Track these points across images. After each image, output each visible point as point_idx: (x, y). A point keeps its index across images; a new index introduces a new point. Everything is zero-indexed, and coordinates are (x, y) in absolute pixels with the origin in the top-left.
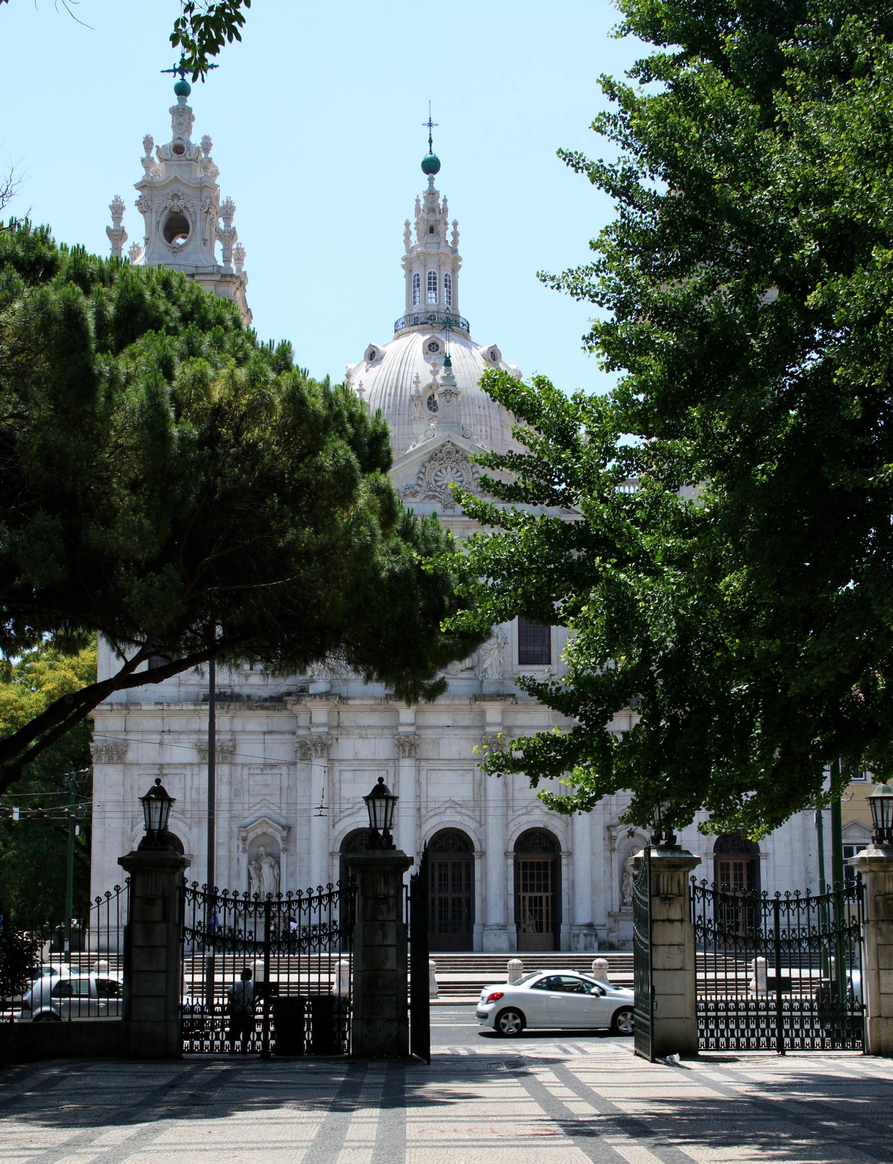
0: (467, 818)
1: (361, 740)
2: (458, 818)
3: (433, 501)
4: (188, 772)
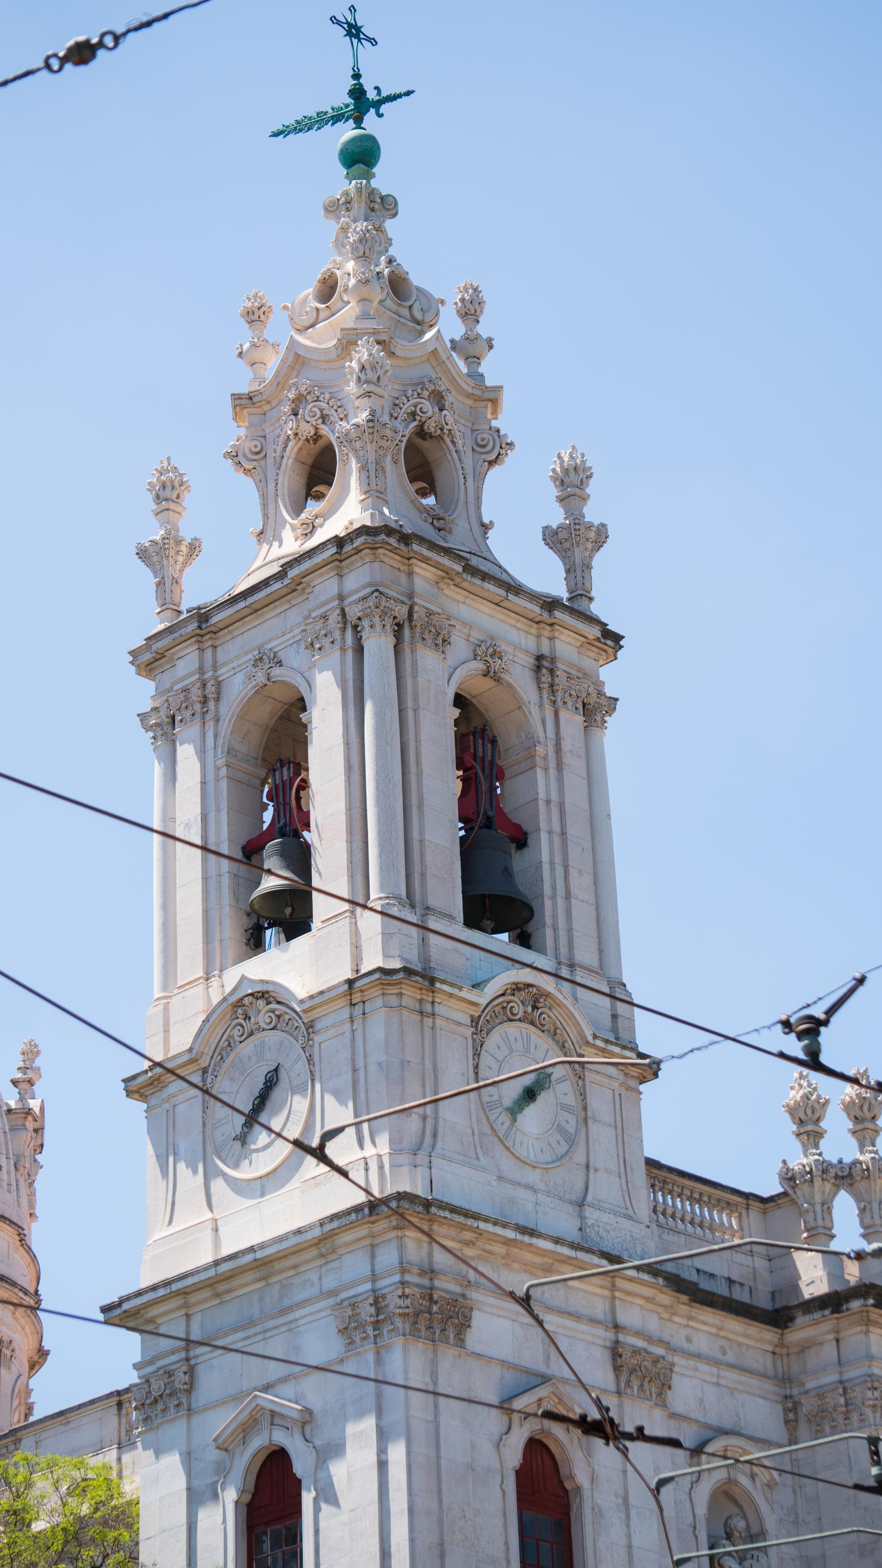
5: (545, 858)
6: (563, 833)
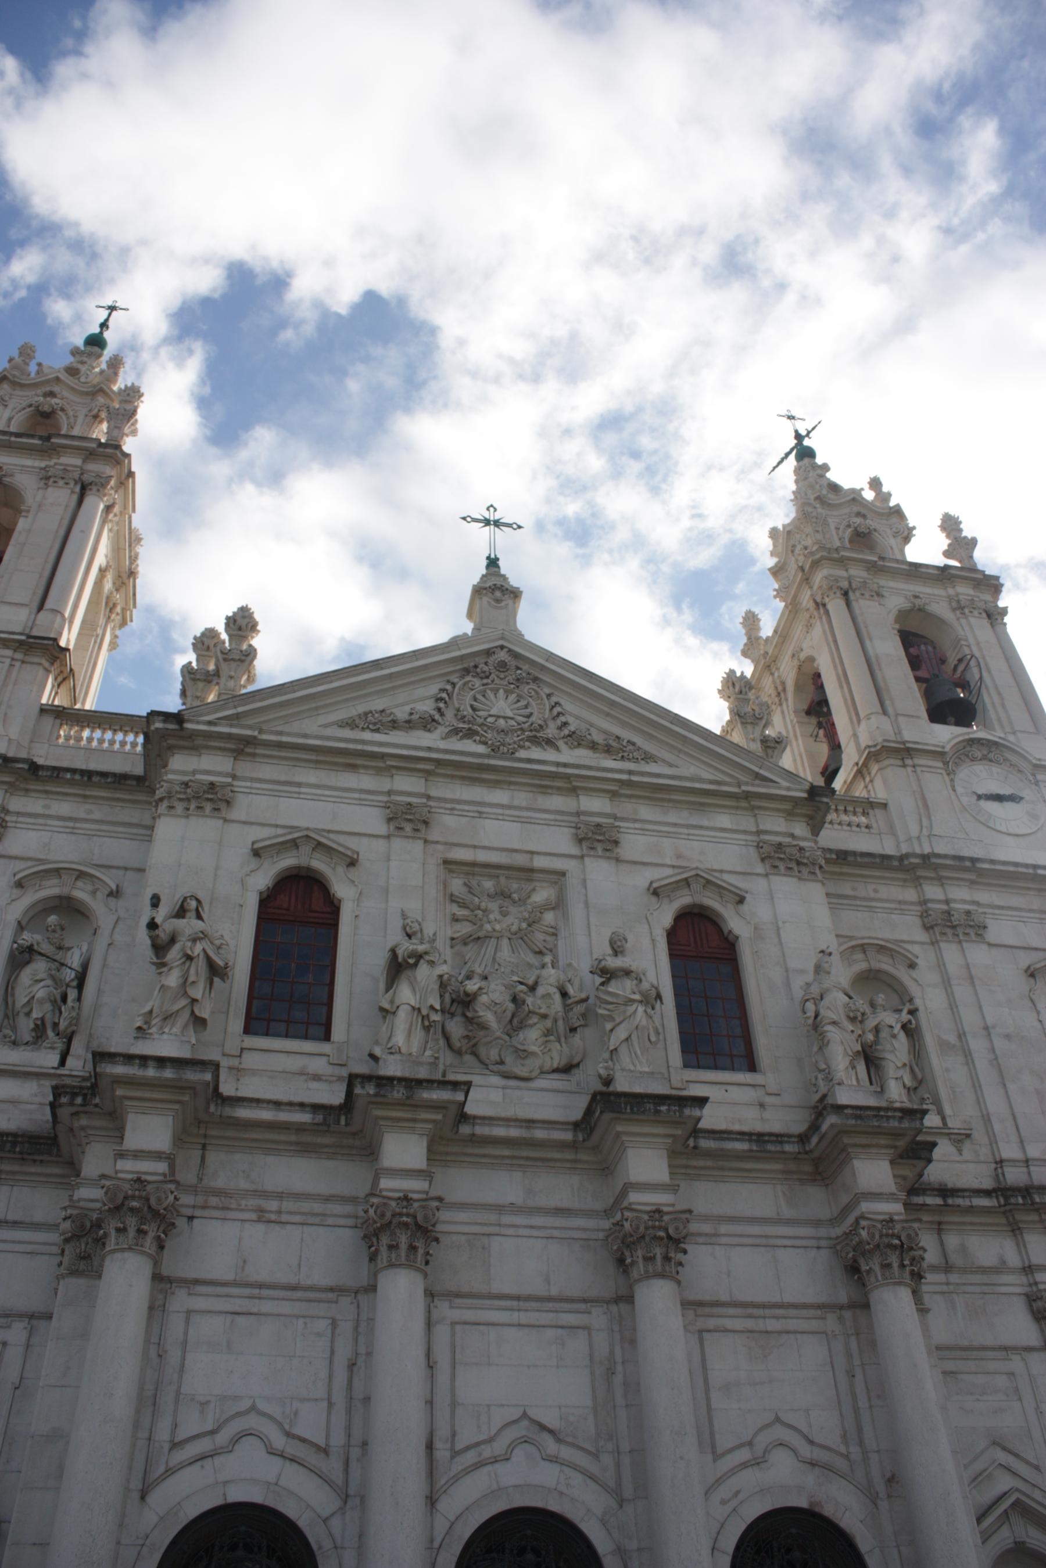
0: (577, 1479)
1: (261, 1227)
2: (548, 1475)
3: (465, 741)
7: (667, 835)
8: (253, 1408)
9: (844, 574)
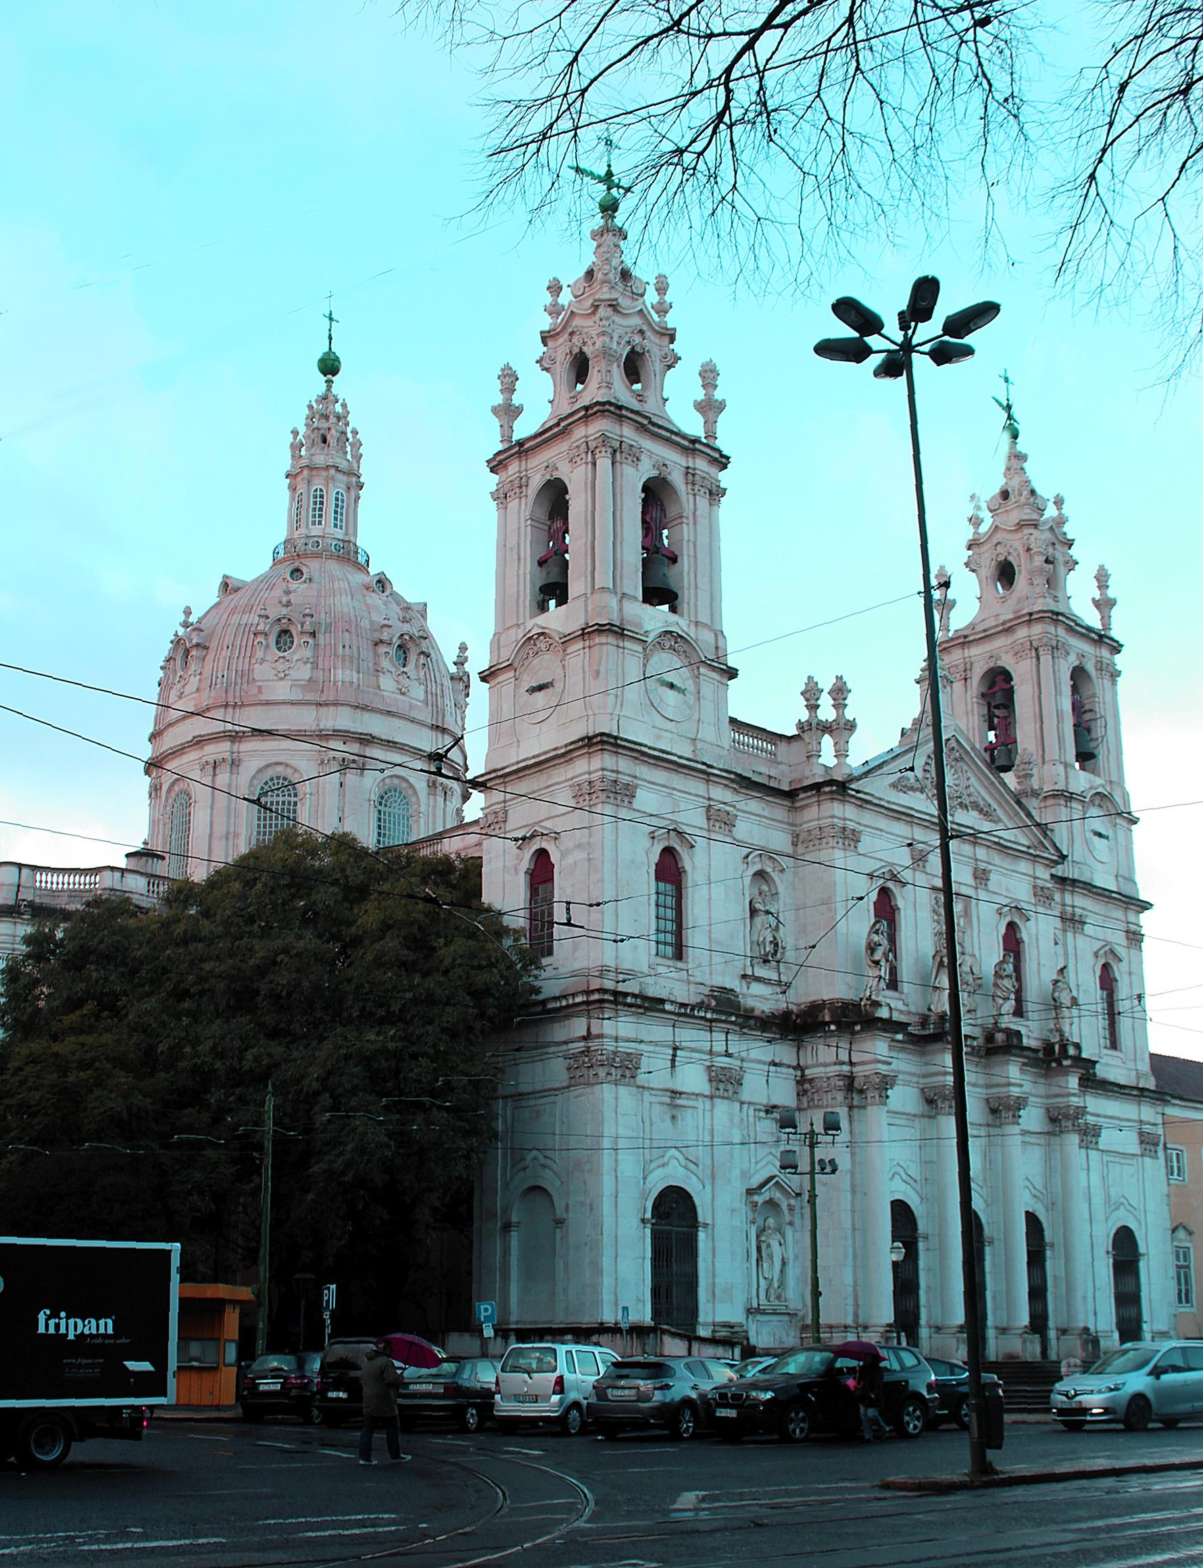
4: (699, 1103)
5: (686, 569)
6: (695, 556)
7: (1004, 875)
8: (898, 1164)
9: (1053, 631)
